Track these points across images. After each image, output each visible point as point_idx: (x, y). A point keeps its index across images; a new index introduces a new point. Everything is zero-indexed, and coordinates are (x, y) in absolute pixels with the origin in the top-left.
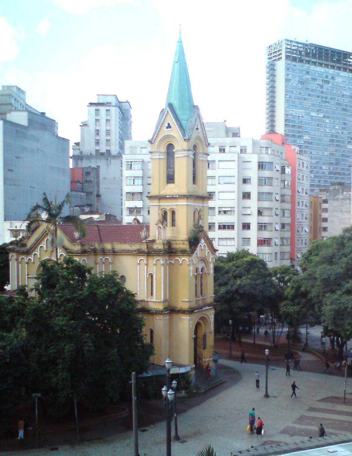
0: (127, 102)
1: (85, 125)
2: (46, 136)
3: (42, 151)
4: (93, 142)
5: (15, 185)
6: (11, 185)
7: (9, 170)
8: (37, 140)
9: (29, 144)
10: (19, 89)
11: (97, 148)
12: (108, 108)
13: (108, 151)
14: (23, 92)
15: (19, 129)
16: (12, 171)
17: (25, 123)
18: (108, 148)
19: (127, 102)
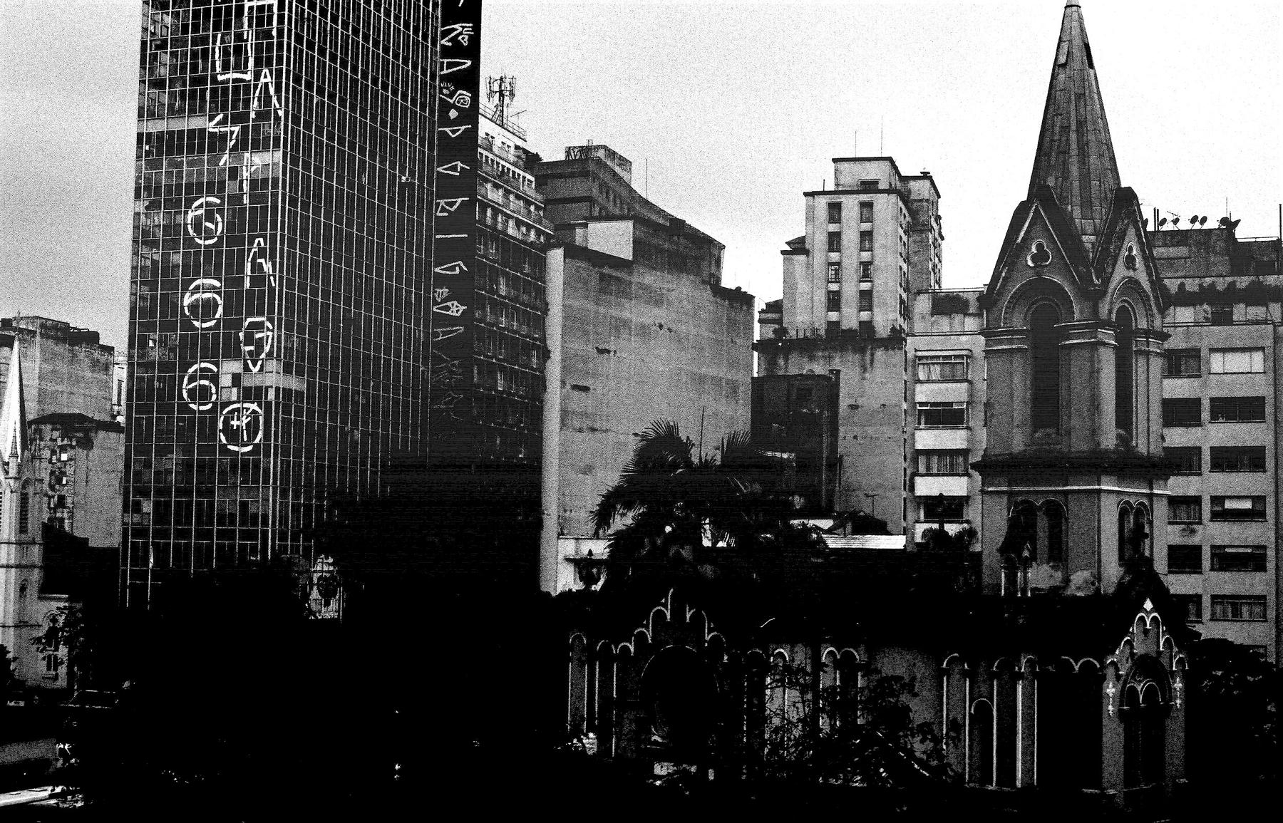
0: (926, 176)
1: (798, 247)
2: (682, 289)
3: (670, 330)
4: (821, 297)
5: (593, 430)
6: (580, 430)
7: (576, 387)
8: (657, 299)
9: (636, 313)
10: (612, 154)
11: (834, 316)
12: (865, 198)
13: (867, 326)
14: (624, 163)
15: (606, 271)
16: (586, 389)
17: (625, 251)
18: (865, 316)
19: (926, 176)
